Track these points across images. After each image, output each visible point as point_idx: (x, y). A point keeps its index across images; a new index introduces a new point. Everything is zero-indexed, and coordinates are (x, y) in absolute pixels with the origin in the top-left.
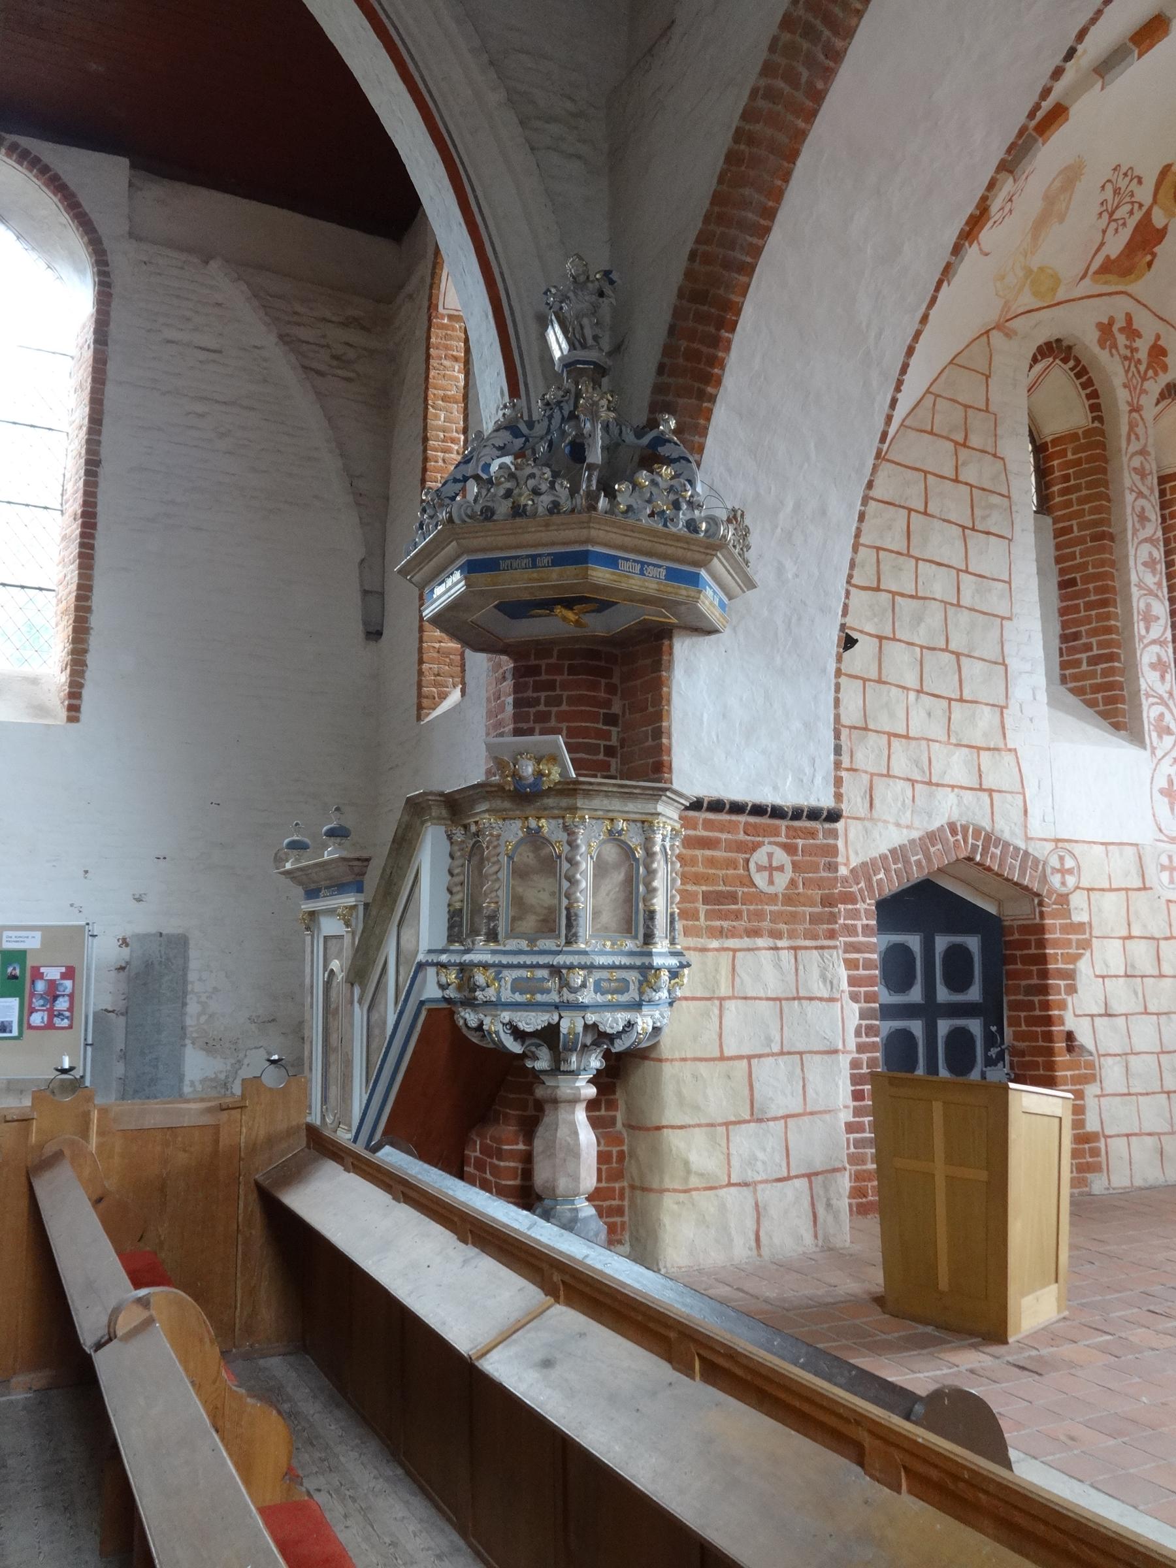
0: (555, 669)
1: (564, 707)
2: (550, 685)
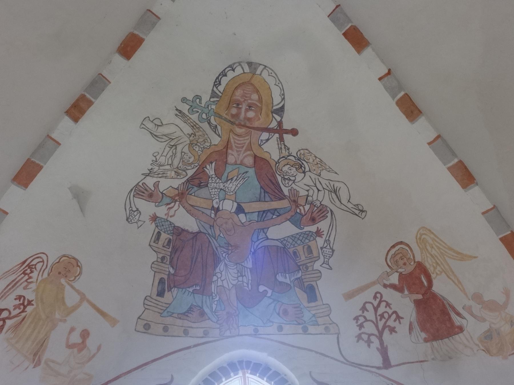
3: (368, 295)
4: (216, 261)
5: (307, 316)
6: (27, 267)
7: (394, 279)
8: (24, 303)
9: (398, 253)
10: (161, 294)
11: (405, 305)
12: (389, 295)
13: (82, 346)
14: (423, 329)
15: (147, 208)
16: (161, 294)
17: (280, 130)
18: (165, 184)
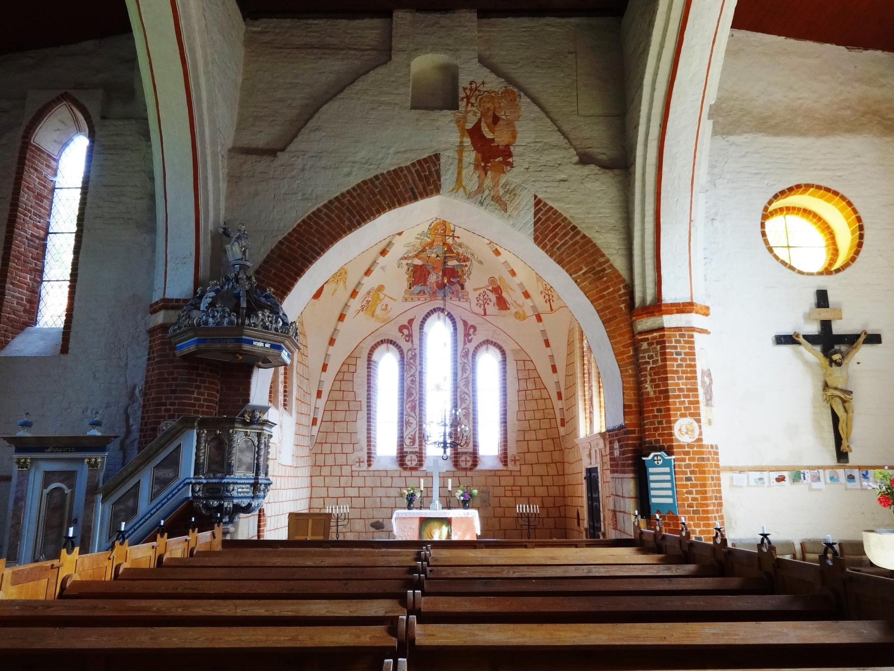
2: (202, 375)
3: (481, 291)
4: (429, 273)
5: (460, 295)
6: (369, 293)
7: (490, 288)
8: (368, 302)
9: (492, 280)
11: (493, 297)
12: (488, 292)
13: (386, 309)
14: (498, 305)
15: (404, 262)
17: (453, 236)
18: (410, 255)
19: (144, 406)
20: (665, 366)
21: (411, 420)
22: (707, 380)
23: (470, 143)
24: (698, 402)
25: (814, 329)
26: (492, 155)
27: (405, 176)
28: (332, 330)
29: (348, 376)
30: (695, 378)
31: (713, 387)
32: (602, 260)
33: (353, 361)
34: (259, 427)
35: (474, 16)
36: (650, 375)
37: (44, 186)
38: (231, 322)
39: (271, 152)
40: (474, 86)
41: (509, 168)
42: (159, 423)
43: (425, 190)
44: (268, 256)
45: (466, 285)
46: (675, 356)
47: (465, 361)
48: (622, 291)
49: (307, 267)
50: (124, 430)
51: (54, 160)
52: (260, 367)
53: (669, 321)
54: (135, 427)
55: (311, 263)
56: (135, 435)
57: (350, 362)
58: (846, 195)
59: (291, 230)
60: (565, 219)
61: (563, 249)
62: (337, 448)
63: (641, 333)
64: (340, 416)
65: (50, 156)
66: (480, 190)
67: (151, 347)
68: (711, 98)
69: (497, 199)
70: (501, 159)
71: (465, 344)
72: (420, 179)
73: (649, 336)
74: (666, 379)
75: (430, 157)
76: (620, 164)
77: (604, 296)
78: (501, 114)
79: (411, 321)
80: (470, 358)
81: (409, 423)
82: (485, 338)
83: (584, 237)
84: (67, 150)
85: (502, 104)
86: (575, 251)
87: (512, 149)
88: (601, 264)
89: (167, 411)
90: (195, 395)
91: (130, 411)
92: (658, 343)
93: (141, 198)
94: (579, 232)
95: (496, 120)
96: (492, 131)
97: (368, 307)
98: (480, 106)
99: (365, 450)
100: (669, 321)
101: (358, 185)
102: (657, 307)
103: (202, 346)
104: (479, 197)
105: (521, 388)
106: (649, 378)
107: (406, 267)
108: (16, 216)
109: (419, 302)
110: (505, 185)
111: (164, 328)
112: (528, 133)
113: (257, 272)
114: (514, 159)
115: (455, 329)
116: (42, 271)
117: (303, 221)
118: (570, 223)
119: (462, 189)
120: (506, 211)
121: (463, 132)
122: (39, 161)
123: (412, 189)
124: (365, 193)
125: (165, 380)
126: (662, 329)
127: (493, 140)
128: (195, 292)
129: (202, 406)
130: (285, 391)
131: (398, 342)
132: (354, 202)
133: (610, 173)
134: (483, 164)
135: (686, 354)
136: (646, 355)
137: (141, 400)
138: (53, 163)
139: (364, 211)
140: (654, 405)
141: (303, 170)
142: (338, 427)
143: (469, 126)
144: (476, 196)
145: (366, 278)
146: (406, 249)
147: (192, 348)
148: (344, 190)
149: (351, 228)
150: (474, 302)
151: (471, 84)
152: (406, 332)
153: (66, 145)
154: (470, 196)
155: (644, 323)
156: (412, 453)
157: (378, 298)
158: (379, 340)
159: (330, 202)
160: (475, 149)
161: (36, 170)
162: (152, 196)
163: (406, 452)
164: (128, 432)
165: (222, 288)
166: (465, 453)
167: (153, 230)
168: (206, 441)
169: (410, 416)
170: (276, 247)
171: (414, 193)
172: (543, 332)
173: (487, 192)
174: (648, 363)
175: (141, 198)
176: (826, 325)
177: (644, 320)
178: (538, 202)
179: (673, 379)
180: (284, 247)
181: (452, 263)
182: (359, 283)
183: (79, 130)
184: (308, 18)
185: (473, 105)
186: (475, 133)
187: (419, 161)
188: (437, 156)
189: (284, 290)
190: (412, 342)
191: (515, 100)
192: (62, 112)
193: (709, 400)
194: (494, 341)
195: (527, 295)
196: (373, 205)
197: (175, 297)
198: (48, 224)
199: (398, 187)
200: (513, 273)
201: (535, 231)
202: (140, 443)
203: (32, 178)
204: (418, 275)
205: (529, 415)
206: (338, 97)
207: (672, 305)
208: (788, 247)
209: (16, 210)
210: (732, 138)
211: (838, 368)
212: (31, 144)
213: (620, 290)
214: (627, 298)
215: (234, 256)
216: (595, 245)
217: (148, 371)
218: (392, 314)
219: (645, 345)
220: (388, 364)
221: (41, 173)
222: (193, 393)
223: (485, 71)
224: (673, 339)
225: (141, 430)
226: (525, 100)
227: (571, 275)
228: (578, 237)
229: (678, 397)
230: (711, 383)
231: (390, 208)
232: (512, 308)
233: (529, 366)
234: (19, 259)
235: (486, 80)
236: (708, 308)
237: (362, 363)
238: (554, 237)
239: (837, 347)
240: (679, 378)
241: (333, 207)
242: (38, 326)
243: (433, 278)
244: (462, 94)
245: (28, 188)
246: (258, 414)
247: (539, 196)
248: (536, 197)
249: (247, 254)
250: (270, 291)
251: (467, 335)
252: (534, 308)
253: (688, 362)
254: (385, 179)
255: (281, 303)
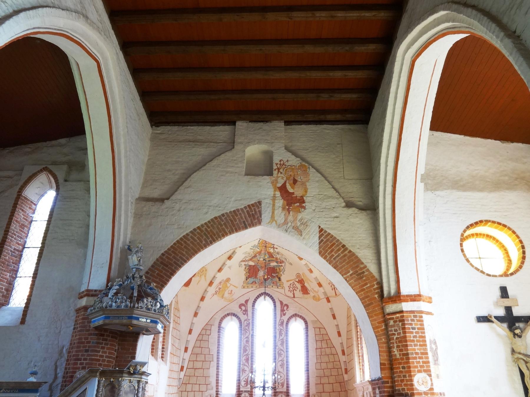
0: (108, 336)
1: (109, 346)
2: (106, 340)
3: (291, 282)
4: (259, 270)
5: (278, 284)
7: (297, 280)
8: (220, 289)
9: (298, 275)
10: (247, 280)
11: (299, 286)
12: (296, 283)
13: (231, 293)
15: (243, 263)
16: (247, 280)
17: (274, 248)
18: (247, 259)
19: (67, 360)
20: (405, 337)
21: (246, 368)
22: (434, 347)
23: (279, 195)
24: (428, 362)
25: (501, 312)
26: (293, 202)
27: (240, 214)
28: (196, 307)
29: (205, 338)
30: (426, 345)
31: (439, 351)
32: (362, 266)
33: (208, 327)
34: (139, 376)
35: (282, 124)
36: (396, 343)
37: (26, 220)
38: (126, 306)
39: (161, 200)
40: (282, 162)
41: (303, 210)
42: (75, 372)
43: (252, 222)
44: (155, 263)
45: (282, 278)
46: (411, 330)
47: (281, 328)
48: (376, 286)
49: (178, 270)
50: (53, 376)
51: (35, 204)
52: (144, 334)
53: (406, 306)
54: (60, 375)
55: (180, 267)
56: (60, 380)
57: (206, 329)
58: (511, 227)
59: (169, 246)
60: (338, 240)
61: (337, 259)
62: (196, 388)
63: (389, 314)
64: (198, 365)
65: (32, 202)
66: (286, 222)
67: (76, 321)
68: (422, 170)
69: (296, 228)
70: (298, 204)
71: (281, 316)
72: (250, 216)
73: (394, 316)
74: (407, 346)
75: (255, 203)
76: (371, 208)
77: (364, 290)
78: (298, 178)
79: (247, 301)
80: (284, 326)
81: (244, 371)
82: (295, 313)
83: (350, 251)
84: (43, 198)
85: (299, 173)
86: (345, 260)
87: (305, 198)
88: (361, 269)
89: (81, 364)
90: (101, 354)
91: (58, 364)
92: (400, 321)
93: (81, 227)
94: (347, 249)
95: (295, 181)
96: (293, 188)
97: (219, 292)
98: (286, 174)
99: (215, 389)
100: (406, 306)
101: (212, 220)
102: (397, 297)
103: (107, 321)
104: (285, 227)
105: (318, 347)
106: (395, 345)
107: (244, 267)
108: (6, 238)
109: (253, 289)
110: (301, 219)
111: (85, 308)
112: (314, 189)
113: (147, 273)
114: (306, 205)
115: (275, 306)
116: (17, 271)
117: (178, 241)
118: (341, 243)
119: (274, 222)
120: (301, 235)
121: (276, 188)
122: (25, 205)
123: (244, 222)
124: (215, 224)
125: (83, 343)
126: (402, 312)
127: (293, 193)
128: (107, 286)
129: (104, 361)
130: (163, 348)
131: (238, 315)
132: (209, 230)
133: (364, 213)
134: (287, 207)
135: (418, 329)
136: (393, 329)
137: (66, 356)
138: (34, 206)
139: (215, 235)
140: (400, 363)
141: (179, 210)
142: (199, 373)
143: (279, 185)
144: (284, 226)
145: (219, 274)
146: (244, 256)
147: (101, 322)
148: (203, 222)
149: (206, 246)
150: (287, 289)
151: (280, 161)
152: (243, 308)
153: (42, 196)
154: (279, 226)
155: (391, 308)
156: (246, 391)
157: (227, 286)
158: (226, 313)
159: (195, 230)
160: (283, 198)
161: (23, 210)
162: (88, 226)
163: (242, 391)
164: (56, 377)
165: (123, 283)
166: (281, 392)
167: (86, 246)
168: (103, 386)
169: (245, 365)
170: (160, 257)
171: (245, 224)
172: (331, 309)
173: (290, 224)
174: (395, 334)
175: (81, 227)
176: (508, 309)
177: (390, 305)
178: (321, 230)
179: (411, 346)
180: (164, 257)
181: (273, 264)
182: (214, 277)
183: (51, 188)
184: (187, 126)
185: (281, 173)
186: (283, 189)
187: (249, 206)
188: (260, 203)
189: (163, 283)
190: (247, 315)
191: (306, 171)
192: (43, 178)
193: (436, 360)
194: (300, 314)
195: (320, 285)
196: (220, 232)
197: (95, 288)
198: (25, 242)
199: (236, 221)
200: (311, 271)
201: (320, 248)
202: (62, 386)
203: (19, 215)
204: (252, 272)
205: (324, 365)
206: (203, 168)
207: (407, 296)
208: (480, 258)
209: (7, 234)
210: (438, 193)
211: (519, 339)
212: (22, 196)
213: (374, 285)
214: (379, 290)
215: (133, 263)
216: (357, 257)
217: (73, 336)
218: (235, 297)
219: (391, 323)
220: (231, 329)
221: (25, 212)
222: (99, 352)
223: (289, 154)
224: (410, 319)
225: (64, 377)
226: (312, 170)
227: (342, 275)
228: (346, 252)
229: (415, 358)
230: (436, 349)
231: (230, 234)
232: (311, 293)
233: (323, 331)
234: (4, 264)
235: (289, 159)
236: (430, 298)
237: (215, 328)
238: (332, 251)
239: (517, 325)
240: (415, 345)
241: (196, 233)
242: (9, 306)
243: (261, 273)
244: (275, 167)
245: (16, 221)
246: (139, 367)
247: (322, 227)
248: (320, 227)
249: (141, 262)
250: (153, 285)
251: (282, 310)
252: (325, 293)
253: (420, 334)
254: (228, 216)
255: (160, 292)
